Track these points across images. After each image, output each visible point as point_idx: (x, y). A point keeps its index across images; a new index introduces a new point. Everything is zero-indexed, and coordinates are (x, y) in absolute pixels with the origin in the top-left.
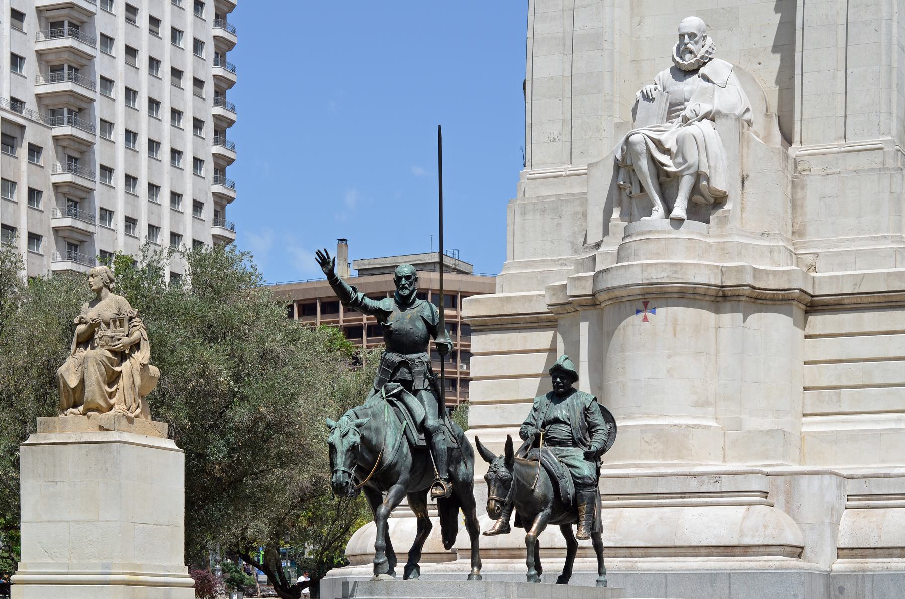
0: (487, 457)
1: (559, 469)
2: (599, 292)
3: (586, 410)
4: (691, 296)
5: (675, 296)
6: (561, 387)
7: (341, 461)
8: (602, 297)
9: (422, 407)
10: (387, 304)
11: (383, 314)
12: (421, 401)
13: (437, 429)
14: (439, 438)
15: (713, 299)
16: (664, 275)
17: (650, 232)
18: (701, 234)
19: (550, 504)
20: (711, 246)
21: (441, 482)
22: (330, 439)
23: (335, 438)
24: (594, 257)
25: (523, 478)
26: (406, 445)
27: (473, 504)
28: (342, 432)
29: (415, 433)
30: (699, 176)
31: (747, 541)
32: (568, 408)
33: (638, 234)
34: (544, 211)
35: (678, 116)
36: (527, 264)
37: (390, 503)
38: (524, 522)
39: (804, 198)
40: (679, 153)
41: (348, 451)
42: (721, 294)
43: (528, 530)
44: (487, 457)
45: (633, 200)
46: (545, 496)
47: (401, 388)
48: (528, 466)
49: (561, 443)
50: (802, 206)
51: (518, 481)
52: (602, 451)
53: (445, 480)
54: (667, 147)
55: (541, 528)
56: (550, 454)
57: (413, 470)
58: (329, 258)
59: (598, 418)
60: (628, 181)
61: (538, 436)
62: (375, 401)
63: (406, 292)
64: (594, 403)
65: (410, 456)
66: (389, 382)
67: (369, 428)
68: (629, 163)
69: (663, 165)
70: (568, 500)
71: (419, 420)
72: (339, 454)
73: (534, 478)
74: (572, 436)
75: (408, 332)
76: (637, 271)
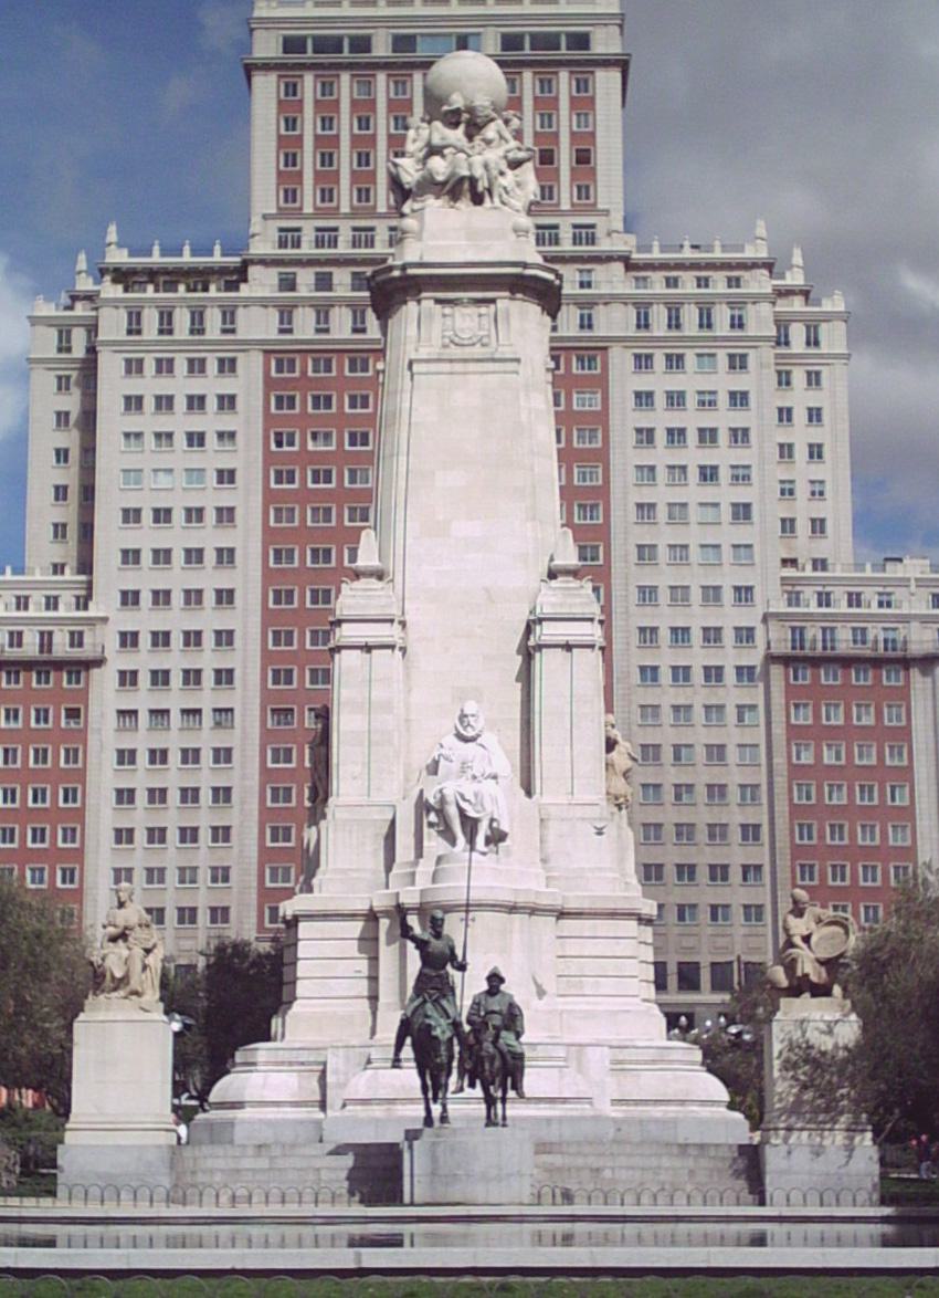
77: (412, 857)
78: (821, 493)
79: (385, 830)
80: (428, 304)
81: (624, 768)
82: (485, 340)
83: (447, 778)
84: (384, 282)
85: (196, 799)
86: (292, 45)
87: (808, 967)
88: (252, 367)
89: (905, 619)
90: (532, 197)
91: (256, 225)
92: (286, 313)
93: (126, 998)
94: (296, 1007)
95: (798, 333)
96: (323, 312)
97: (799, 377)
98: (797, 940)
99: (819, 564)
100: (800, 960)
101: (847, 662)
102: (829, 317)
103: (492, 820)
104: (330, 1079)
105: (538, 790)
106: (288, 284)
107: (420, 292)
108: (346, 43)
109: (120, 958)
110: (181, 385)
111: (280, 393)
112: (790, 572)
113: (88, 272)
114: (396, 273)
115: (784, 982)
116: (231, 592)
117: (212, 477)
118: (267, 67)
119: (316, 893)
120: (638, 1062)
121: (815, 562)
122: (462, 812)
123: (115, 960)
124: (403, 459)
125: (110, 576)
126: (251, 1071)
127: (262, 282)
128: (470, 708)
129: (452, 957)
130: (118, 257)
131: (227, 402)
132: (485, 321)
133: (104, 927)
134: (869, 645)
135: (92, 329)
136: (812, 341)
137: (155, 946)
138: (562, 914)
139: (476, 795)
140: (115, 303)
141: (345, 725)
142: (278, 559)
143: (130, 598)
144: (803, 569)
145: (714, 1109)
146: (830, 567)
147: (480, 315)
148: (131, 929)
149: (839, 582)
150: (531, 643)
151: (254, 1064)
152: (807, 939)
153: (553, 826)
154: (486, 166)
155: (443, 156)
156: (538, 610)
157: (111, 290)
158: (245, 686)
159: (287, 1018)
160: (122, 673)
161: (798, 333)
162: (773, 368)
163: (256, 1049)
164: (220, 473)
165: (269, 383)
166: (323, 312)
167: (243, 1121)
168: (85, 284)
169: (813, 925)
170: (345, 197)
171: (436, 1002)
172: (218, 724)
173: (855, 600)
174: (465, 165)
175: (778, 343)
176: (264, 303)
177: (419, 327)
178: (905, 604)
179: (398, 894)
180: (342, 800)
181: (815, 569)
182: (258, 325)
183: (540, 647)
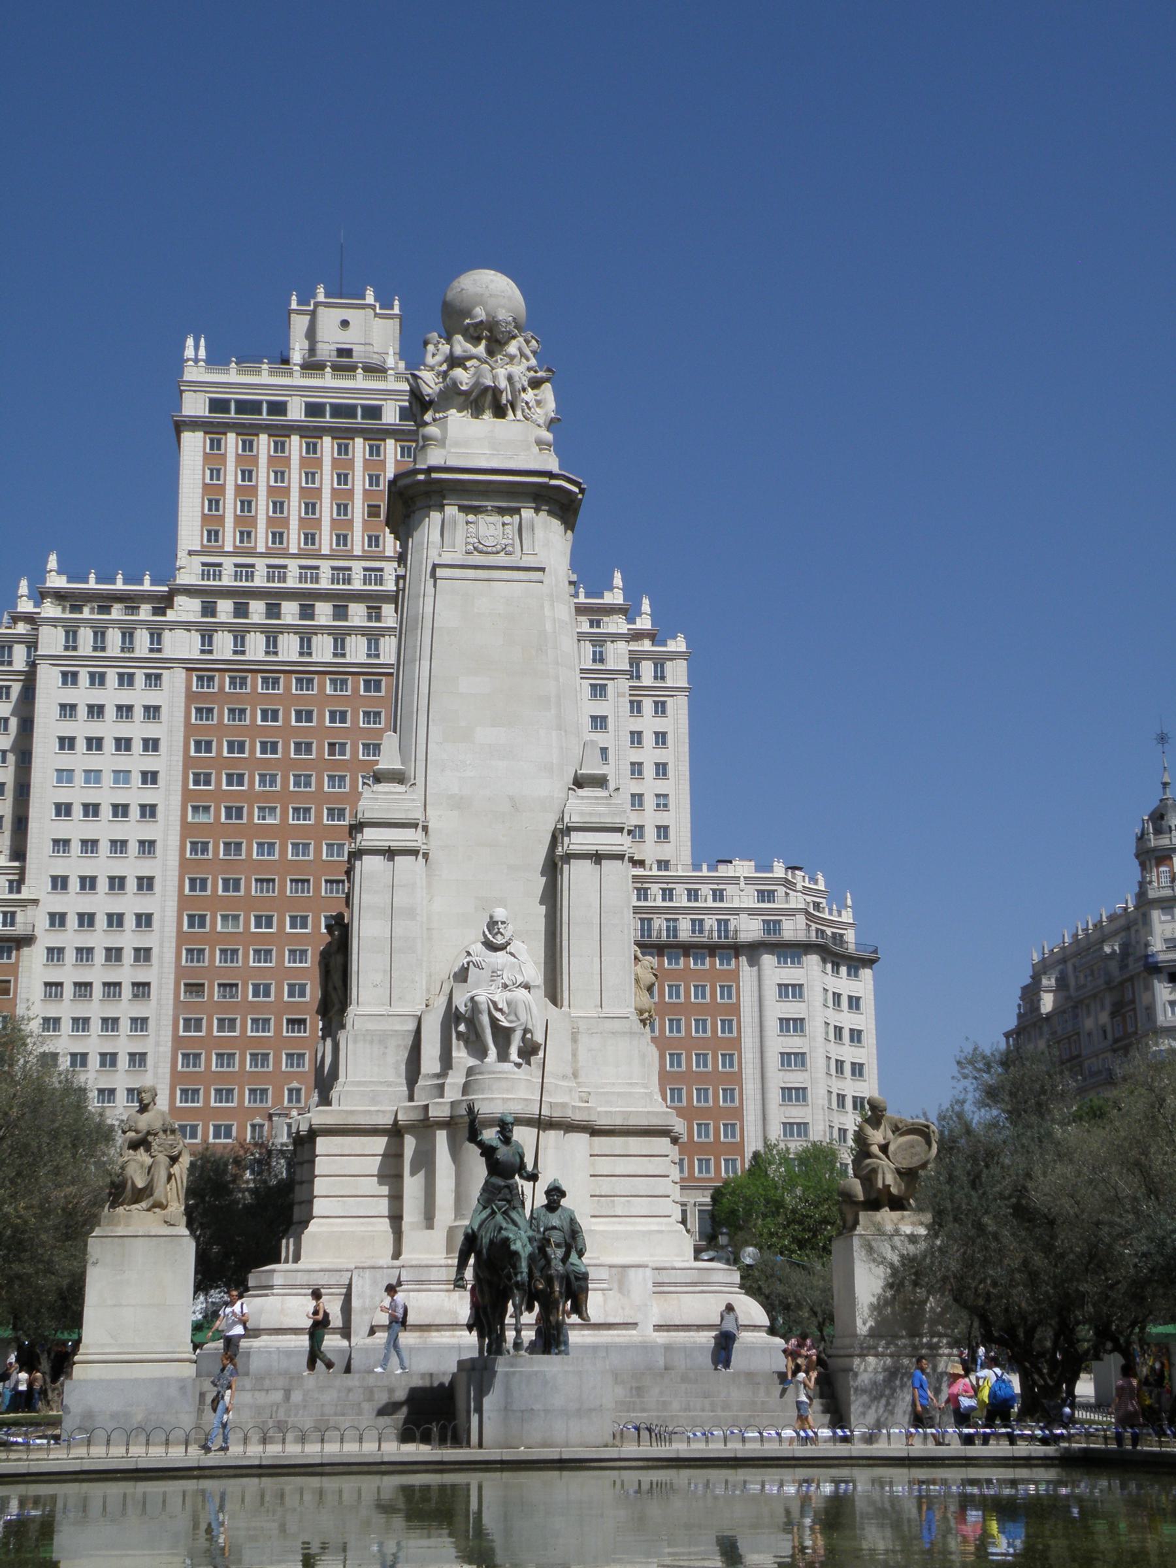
31: (611, 1320)
33: (490, 1073)
34: (372, 1042)
36: (359, 1083)
76: (500, 1102)
77: (437, 1069)
78: (665, 805)
79: (409, 1042)
80: (451, 511)
81: (648, 983)
82: (509, 548)
83: (477, 985)
84: (407, 487)
85: (113, 1063)
86: (218, 405)
87: (888, 1178)
88: (175, 681)
89: (736, 911)
90: (553, 415)
91: (182, 559)
92: (207, 637)
93: (148, 1210)
94: (313, 1227)
95: (647, 668)
96: (239, 637)
97: (648, 705)
98: (875, 1149)
99: (664, 864)
100: (880, 1171)
101: (687, 949)
102: (673, 656)
103: (526, 1031)
104: (356, 1303)
105: (566, 1003)
106: (209, 610)
107: (444, 497)
108: (265, 406)
109: (142, 1166)
110: (111, 695)
111: (200, 706)
112: (639, 871)
113: (29, 598)
114: (421, 477)
115: (861, 1196)
116: (151, 879)
117: (136, 779)
118: (195, 424)
119: (335, 1107)
120: (675, 1284)
121: (659, 862)
122: (494, 1021)
123: (136, 1168)
124: (425, 664)
125: (42, 862)
126: (267, 1295)
127: (187, 608)
128: (500, 913)
129: (522, 1166)
130: (57, 581)
131: (152, 712)
132: (508, 529)
133: (124, 1132)
134: (707, 934)
135: (32, 644)
136: (660, 675)
137: (180, 1154)
138: (595, 1132)
139: (509, 1004)
140: (54, 622)
141: (367, 932)
142: (194, 850)
143: (60, 883)
144: (651, 869)
145: (756, 1334)
146: (672, 867)
147: (504, 524)
148: (156, 1134)
149: (680, 879)
150: (559, 851)
151: (271, 1287)
152: (884, 1148)
153: (583, 1039)
154: (510, 378)
155: (466, 368)
156: (566, 820)
157: (50, 610)
158: (161, 958)
159: (305, 1237)
160: (50, 950)
161: (647, 668)
162: (628, 698)
163: (274, 1271)
164: (144, 774)
165: (190, 697)
166: (239, 637)
167: (259, 1351)
168: (25, 606)
169: (890, 1133)
170: (262, 539)
171: (505, 1213)
172: (135, 996)
173: (693, 895)
174: (489, 376)
175: (632, 678)
176: (187, 626)
177: (443, 534)
178: (736, 899)
179: (426, 1107)
180: (363, 1009)
181: (659, 869)
182: (182, 645)
183: (569, 857)
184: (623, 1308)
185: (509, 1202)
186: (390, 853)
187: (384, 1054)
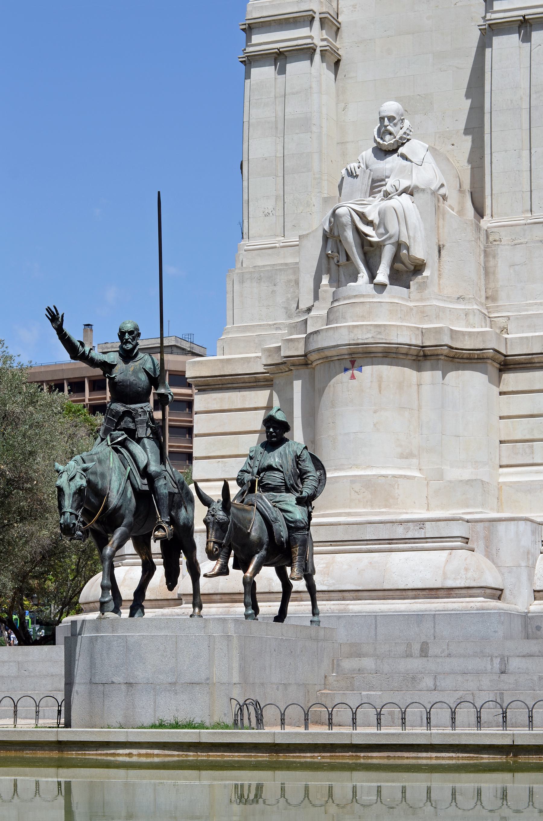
0: (206, 501)
1: (273, 513)
2: (310, 352)
3: (298, 458)
4: (394, 355)
5: (380, 355)
6: (274, 437)
7: (68, 503)
8: (313, 357)
9: (145, 454)
10: (113, 358)
11: (108, 367)
12: (144, 448)
13: (158, 475)
14: (160, 483)
15: (414, 358)
16: (369, 335)
17: (355, 296)
18: (403, 299)
19: (265, 546)
20: (411, 309)
21: (163, 525)
22: (58, 483)
23: (62, 481)
24: (306, 321)
25: (240, 522)
26: (130, 489)
27: (193, 547)
28: (69, 476)
29: (138, 479)
30: (399, 245)
32: (281, 456)
33: (345, 299)
35: (380, 191)
37: (115, 545)
38: (241, 564)
39: (496, 266)
40: (380, 225)
41: (75, 493)
42: (422, 353)
43: (245, 571)
44: (206, 501)
45: (341, 268)
46: (260, 539)
47: (125, 436)
48: (244, 510)
49: (275, 489)
50: (494, 273)
51: (235, 524)
52: (313, 497)
53: (167, 522)
54: (370, 218)
55: (257, 570)
56: (265, 500)
57: (136, 513)
58: (58, 314)
59: (309, 466)
60: (335, 250)
61: (253, 482)
62: (102, 448)
63: (130, 346)
64: (305, 452)
65: (134, 500)
66: (114, 430)
67: (94, 473)
68: (336, 234)
69: (367, 235)
70: (282, 542)
71: (142, 466)
72: (66, 497)
73: (250, 521)
74: (285, 483)
75: (131, 383)
76: (345, 332)
105: (488, 211)
184: (466, 569)
185: (128, 431)
186: (280, 58)
187: (273, 292)
